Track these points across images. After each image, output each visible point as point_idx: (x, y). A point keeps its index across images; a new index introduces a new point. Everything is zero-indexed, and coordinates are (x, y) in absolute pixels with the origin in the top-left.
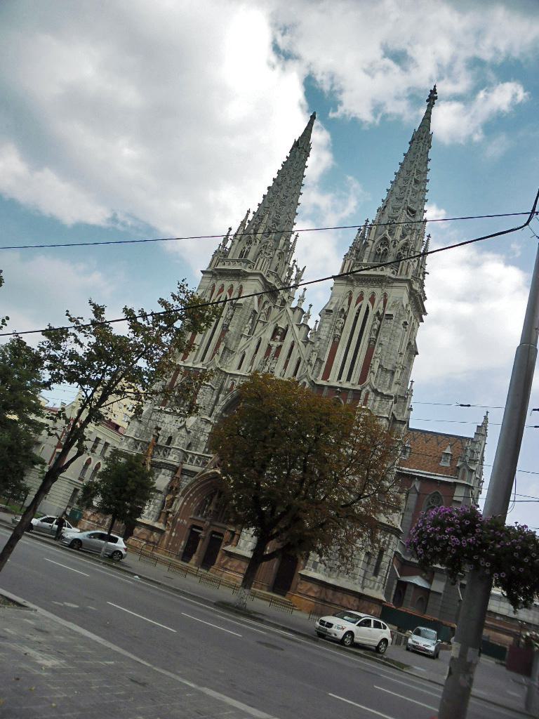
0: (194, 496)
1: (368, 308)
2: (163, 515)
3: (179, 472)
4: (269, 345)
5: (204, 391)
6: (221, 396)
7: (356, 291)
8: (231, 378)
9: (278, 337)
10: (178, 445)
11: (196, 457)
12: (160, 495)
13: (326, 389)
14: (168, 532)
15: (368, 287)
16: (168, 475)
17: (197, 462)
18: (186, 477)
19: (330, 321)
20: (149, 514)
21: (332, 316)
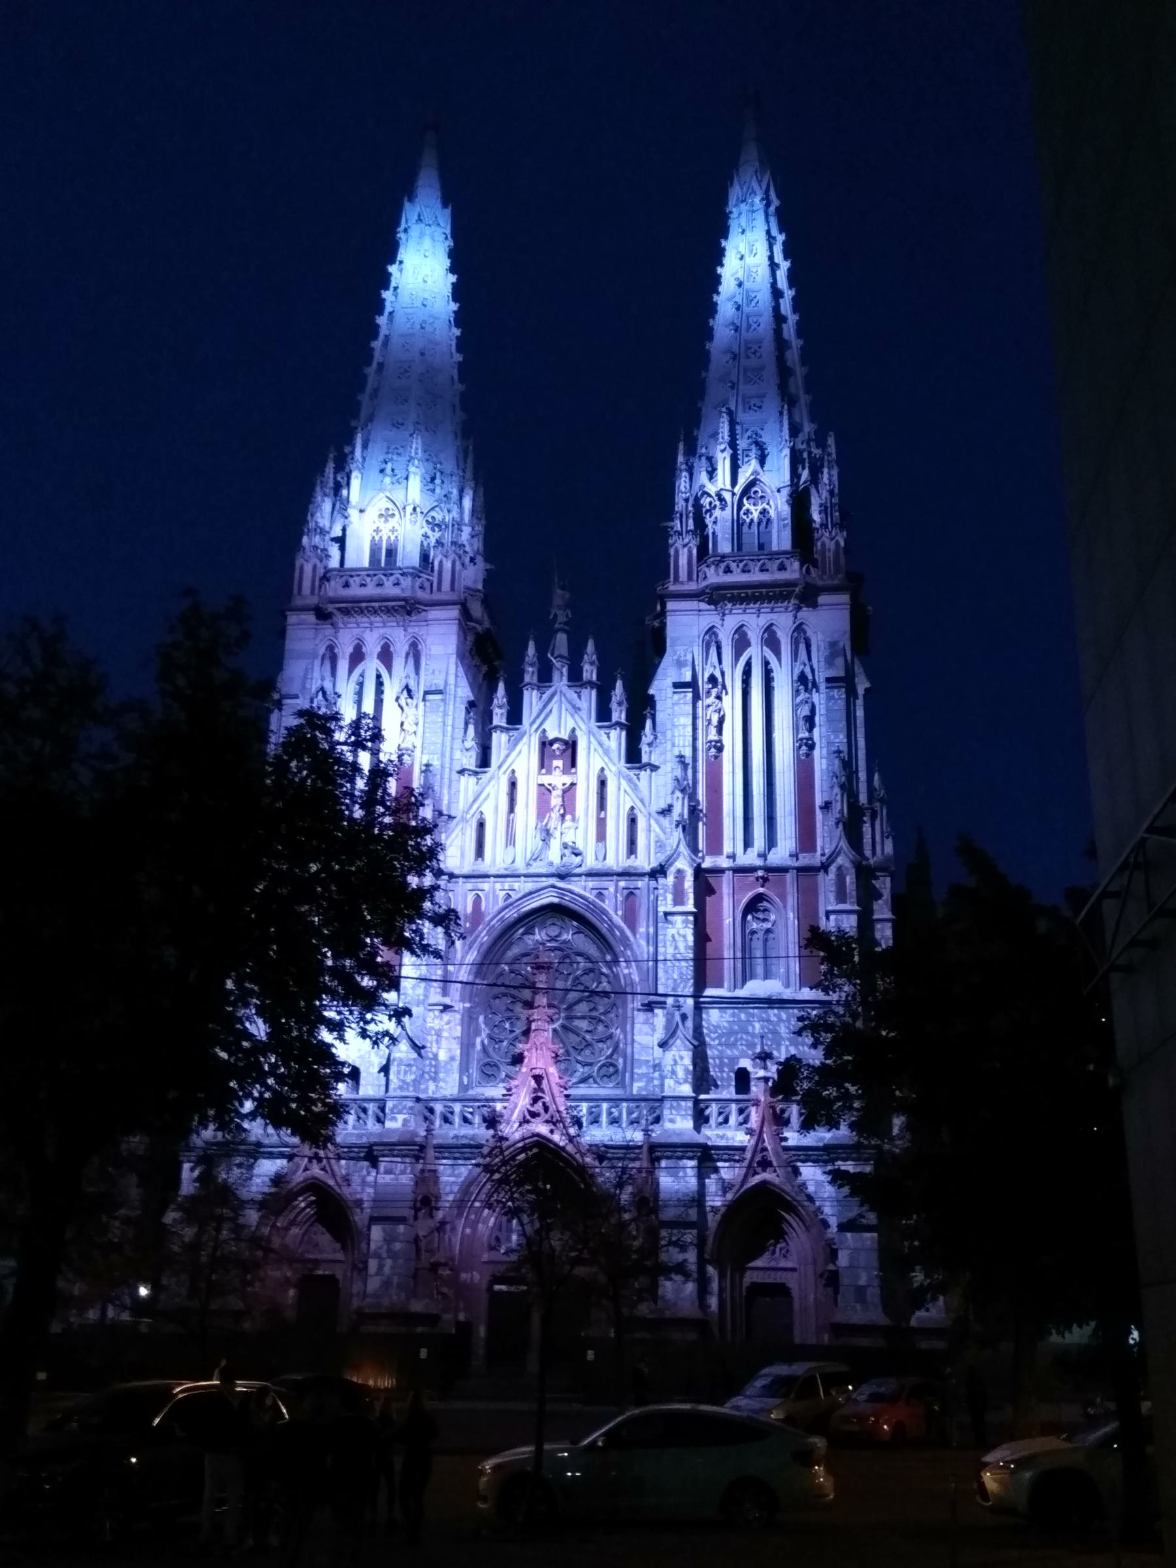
1: (766, 663)
3: (431, 1153)
4: (543, 785)
8: (469, 886)
9: (558, 763)
12: (401, 1228)
16: (403, 1172)
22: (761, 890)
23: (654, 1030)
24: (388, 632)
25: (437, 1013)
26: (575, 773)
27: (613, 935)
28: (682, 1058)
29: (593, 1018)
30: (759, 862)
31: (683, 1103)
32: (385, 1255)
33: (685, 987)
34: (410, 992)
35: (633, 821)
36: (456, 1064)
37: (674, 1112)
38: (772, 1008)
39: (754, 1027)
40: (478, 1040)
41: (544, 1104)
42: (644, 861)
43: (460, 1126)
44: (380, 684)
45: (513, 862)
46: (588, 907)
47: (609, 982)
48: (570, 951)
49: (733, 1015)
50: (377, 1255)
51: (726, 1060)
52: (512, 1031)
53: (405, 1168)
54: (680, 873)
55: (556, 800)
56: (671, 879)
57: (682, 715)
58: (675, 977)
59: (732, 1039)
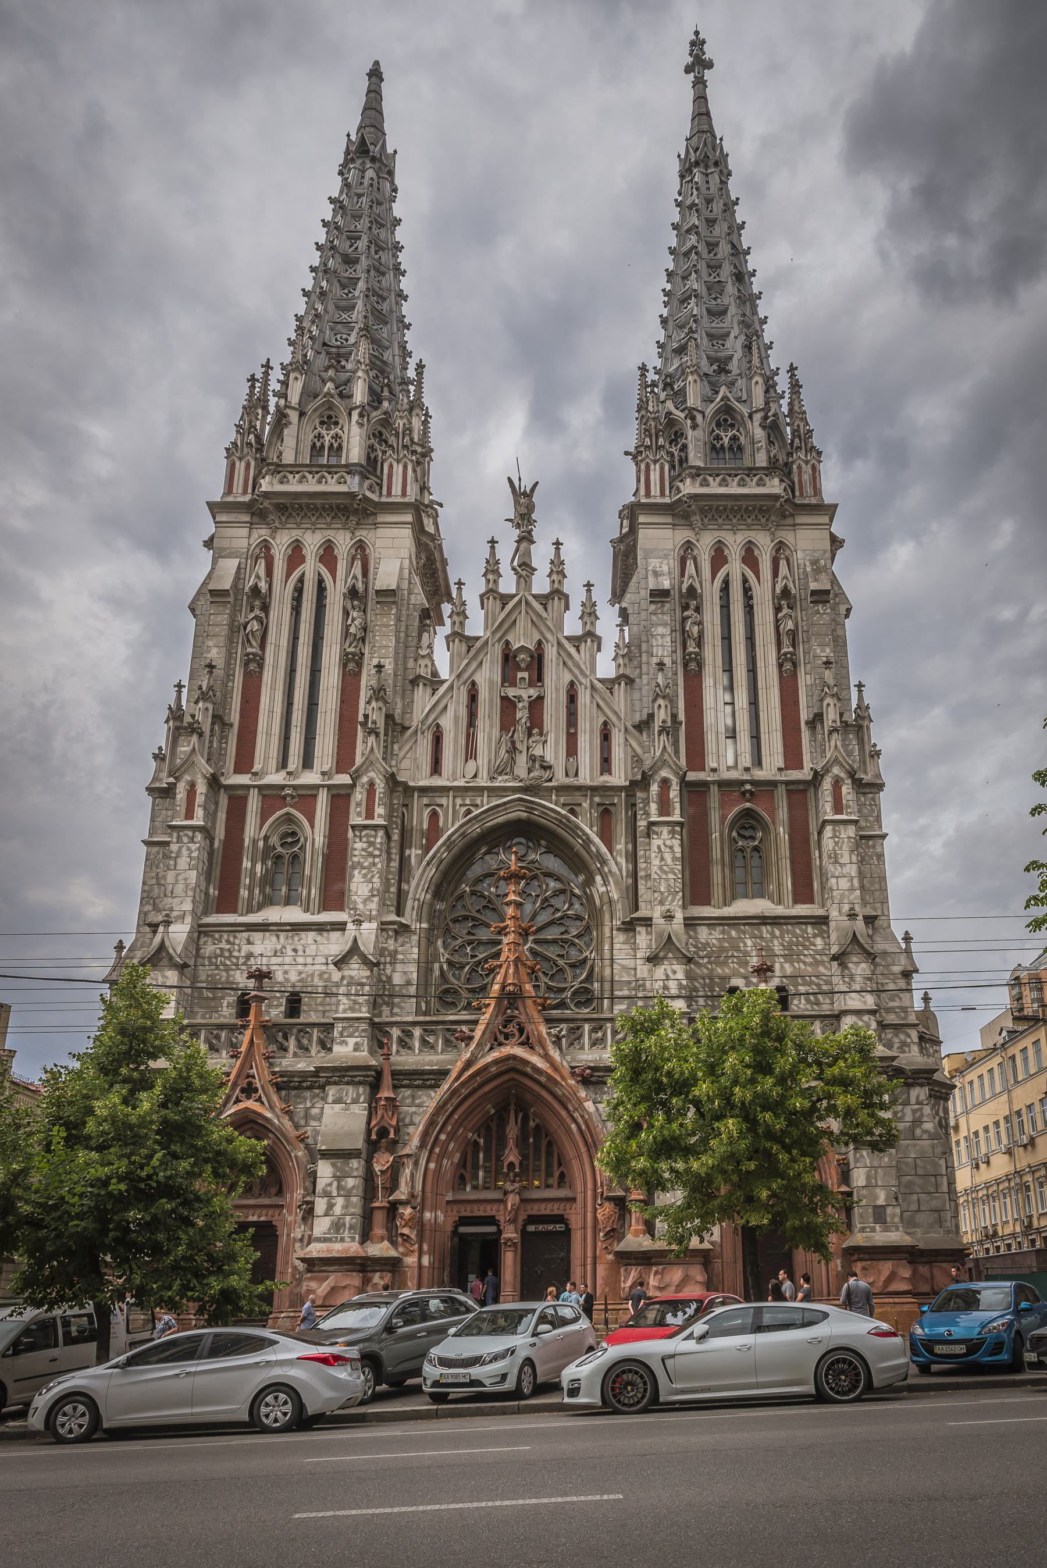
0: (451, 1137)
1: (745, 580)
2: (379, 1218)
3: (387, 1079)
4: (505, 699)
5: (371, 844)
6: (414, 853)
7: (705, 543)
8: (425, 801)
10: (352, 1009)
11: (417, 1032)
13: (714, 790)
14: (411, 1260)
15: (734, 530)
16: (355, 1101)
17: (424, 1042)
18: (408, 1092)
19: (667, 618)
20: (337, 1226)
21: (667, 605)
23: (635, 949)
25: (390, 933)
26: (543, 686)
27: (589, 852)
28: (674, 972)
29: (565, 941)
30: (746, 777)
32: (335, 1194)
33: (673, 901)
34: (360, 906)
35: (606, 737)
36: (412, 990)
40: (436, 966)
41: (519, 1024)
42: (618, 777)
43: (420, 1051)
45: (475, 776)
46: (561, 821)
48: (538, 872)
50: (327, 1194)
52: (473, 957)
53: (359, 1096)
54: (665, 783)
55: (522, 714)
56: (654, 788)
57: (660, 625)
58: (662, 889)
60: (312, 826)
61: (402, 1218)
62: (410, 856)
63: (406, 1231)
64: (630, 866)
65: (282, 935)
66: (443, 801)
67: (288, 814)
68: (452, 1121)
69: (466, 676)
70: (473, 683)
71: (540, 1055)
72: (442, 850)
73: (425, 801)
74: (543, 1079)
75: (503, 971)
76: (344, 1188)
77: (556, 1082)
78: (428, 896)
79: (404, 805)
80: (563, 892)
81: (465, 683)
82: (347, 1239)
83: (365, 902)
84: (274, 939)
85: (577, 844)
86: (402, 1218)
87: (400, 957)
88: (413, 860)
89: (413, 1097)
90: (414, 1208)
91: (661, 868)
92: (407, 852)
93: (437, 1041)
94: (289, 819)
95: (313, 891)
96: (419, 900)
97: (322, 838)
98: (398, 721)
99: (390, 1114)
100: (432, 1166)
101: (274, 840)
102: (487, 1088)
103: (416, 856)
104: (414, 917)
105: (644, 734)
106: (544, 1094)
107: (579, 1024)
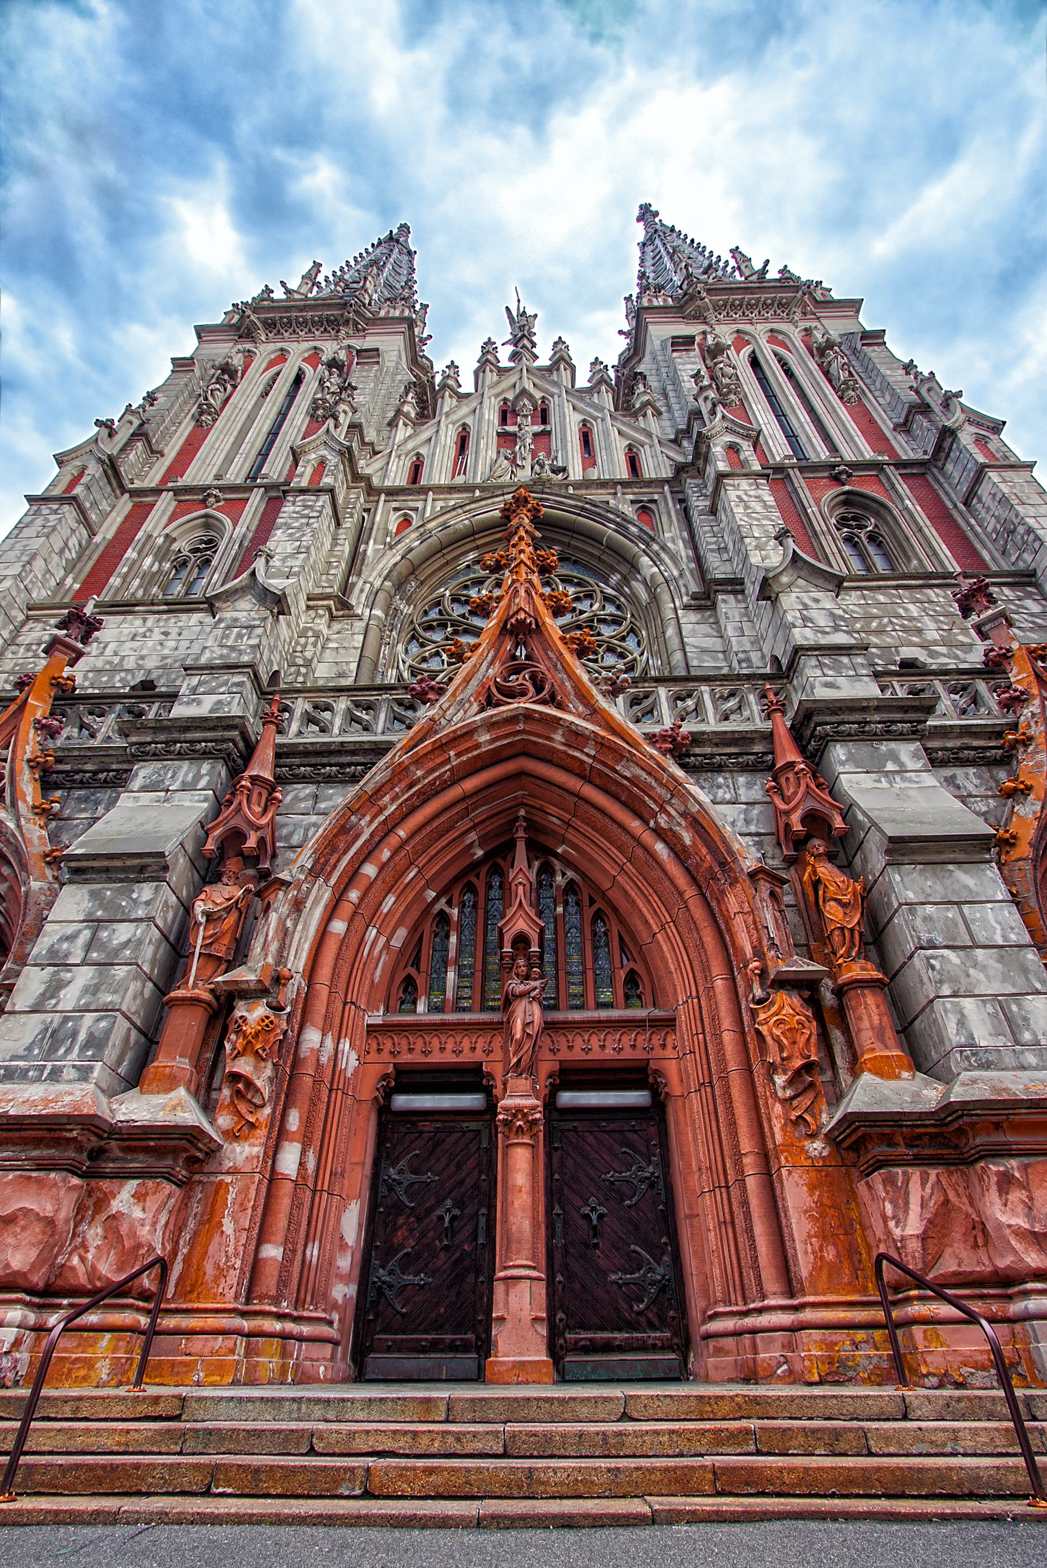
6: (371, 548)
8: (395, 505)
11: (342, 704)
18: (309, 789)
22: (847, 488)
24: (318, 344)
25: (321, 612)
31: (845, 660)
37: (831, 673)
38: (931, 586)
39: (906, 610)
44: (298, 380)
46: (582, 509)
47: (618, 607)
49: (864, 597)
51: (874, 650)
53: (198, 777)
56: (717, 450)
59: (874, 624)
60: (235, 525)
61: (239, 1031)
62: (365, 551)
63: (244, 1066)
64: (690, 553)
65: (151, 619)
66: (420, 505)
67: (206, 516)
68: (393, 841)
69: (454, 417)
70: (465, 427)
71: (579, 716)
72: (414, 535)
73: (395, 505)
74: (586, 755)
75: (504, 603)
76: (102, 946)
77: (619, 755)
78: (388, 584)
79: (365, 510)
80: (589, 596)
81: (454, 423)
82: (70, 1073)
83: (284, 560)
84: (138, 622)
85: (609, 531)
86: (239, 1031)
87: (331, 645)
88: (369, 552)
89: (316, 797)
90: (278, 1008)
91: (748, 515)
92: (362, 547)
93: (376, 718)
94: (208, 523)
95: (216, 576)
96: (372, 585)
97: (244, 529)
98: (367, 440)
99: (258, 809)
100: (339, 926)
101: (183, 545)
102: (470, 784)
103: (376, 551)
104: (363, 599)
105: (685, 443)
106: (589, 791)
107: (647, 687)
